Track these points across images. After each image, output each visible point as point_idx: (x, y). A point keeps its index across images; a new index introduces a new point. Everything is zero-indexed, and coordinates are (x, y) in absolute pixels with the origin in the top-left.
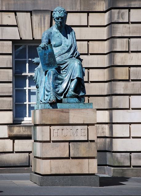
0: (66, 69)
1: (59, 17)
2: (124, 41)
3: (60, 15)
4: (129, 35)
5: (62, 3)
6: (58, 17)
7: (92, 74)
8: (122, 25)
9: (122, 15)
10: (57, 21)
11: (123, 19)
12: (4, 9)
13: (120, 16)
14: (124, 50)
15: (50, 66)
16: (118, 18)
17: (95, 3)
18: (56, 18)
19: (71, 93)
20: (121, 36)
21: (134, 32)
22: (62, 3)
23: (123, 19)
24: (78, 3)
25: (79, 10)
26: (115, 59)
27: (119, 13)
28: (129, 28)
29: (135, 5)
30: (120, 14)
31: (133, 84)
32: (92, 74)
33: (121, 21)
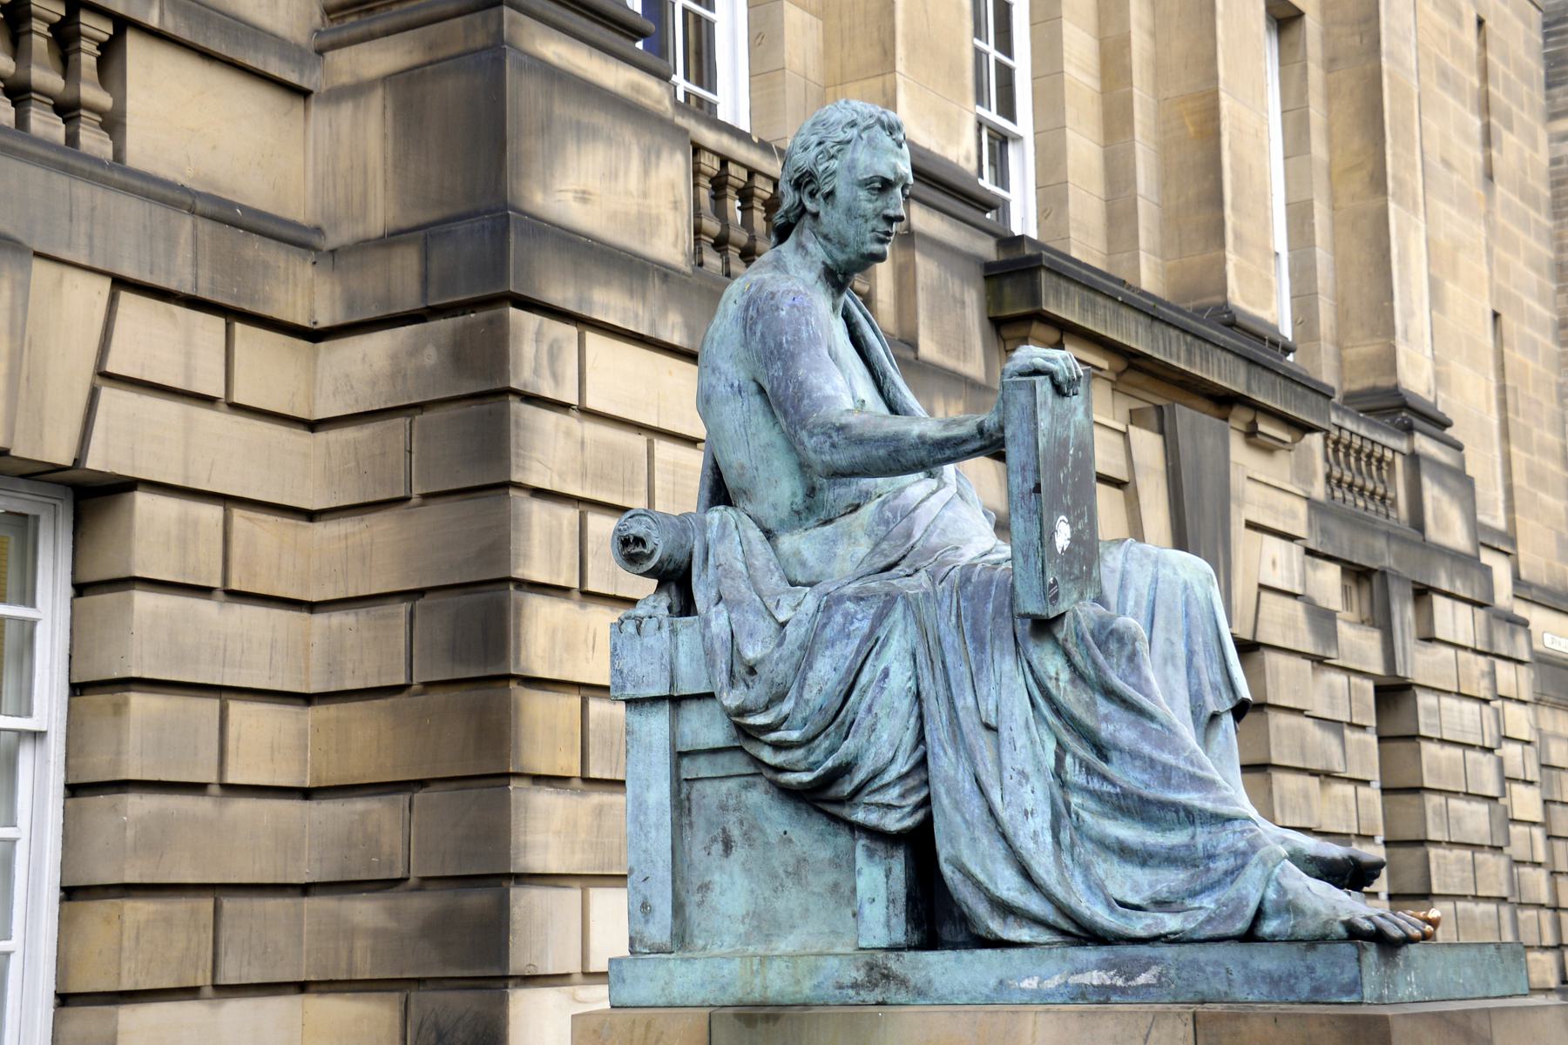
2: (561, 525)
5: (93, 209)
6: (891, 177)
7: (238, 740)
8: (549, 418)
17: (266, 265)
18: (866, 184)
21: (601, 477)
22: (93, 209)
23: (556, 378)
24: (182, 241)
25: (187, 289)
26: (523, 631)
29: (606, 308)
30: (545, 348)
32: (238, 740)
33: (548, 392)
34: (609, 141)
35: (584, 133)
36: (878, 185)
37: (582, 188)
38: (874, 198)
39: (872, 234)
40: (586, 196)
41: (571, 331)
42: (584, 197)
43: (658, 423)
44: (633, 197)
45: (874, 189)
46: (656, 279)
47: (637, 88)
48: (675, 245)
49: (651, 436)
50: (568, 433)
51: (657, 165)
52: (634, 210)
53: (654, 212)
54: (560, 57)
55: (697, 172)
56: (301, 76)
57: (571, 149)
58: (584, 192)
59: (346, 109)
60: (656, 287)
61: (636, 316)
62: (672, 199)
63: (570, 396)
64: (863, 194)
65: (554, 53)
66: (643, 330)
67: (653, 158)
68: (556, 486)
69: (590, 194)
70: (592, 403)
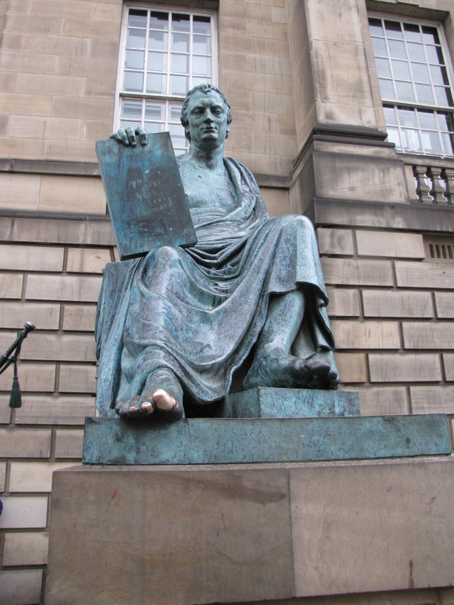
0: (238, 263)
1: (203, 103)
3: (206, 100)
4: (358, 282)
6: (201, 105)
8: (340, 261)
9: (340, 240)
10: (197, 121)
11: (342, 247)
12: (89, 242)
13: (336, 241)
14: (351, 315)
15: (159, 230)
16: (332, 245)
19: (275, 365)
20: (340, 283)
23: (342, 247)
27: (332, 235)
28: (357, 267)
31: (378, 393)
34: (363, 170)
35: (349, 170)
36: (197, 111)
37: (351, 186)
38: (198, 116)
39: (203, 131)
40: (354, 188)
41: (350, 232)
42: (352, 189)
43: (396, 255)
44: (377, 185)
45: (196, 113)
46: (388, 209)
47: (379, 152)
48: (400, 196)
49: (393, 260)
50: (349, 265)
51: (388, 173)
52: (378, 189)
53: (388, 188)
54: (340, 150)
55: (416, 175)
56: (284, 183)
57: (346, 176)
58: (353, 187)
59: (294, 188)
60: (388, 212)
61: (379, 222)
62: (397, 182)
63: (349, 251)
64: (194, 117)
65: (338, 150)
66: (384, 225)
67: (386, 171)
68: (345, 283)
69: (355, 187)
70: (360, 253)
